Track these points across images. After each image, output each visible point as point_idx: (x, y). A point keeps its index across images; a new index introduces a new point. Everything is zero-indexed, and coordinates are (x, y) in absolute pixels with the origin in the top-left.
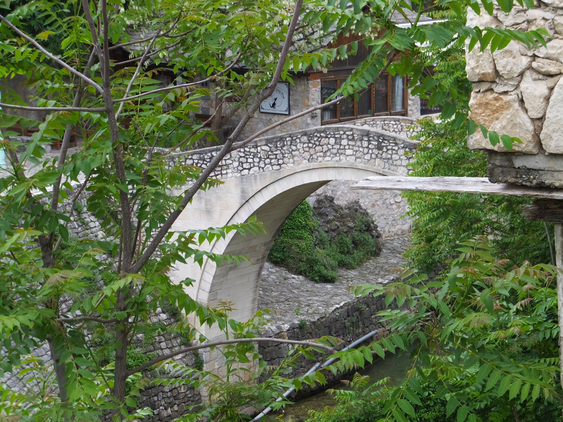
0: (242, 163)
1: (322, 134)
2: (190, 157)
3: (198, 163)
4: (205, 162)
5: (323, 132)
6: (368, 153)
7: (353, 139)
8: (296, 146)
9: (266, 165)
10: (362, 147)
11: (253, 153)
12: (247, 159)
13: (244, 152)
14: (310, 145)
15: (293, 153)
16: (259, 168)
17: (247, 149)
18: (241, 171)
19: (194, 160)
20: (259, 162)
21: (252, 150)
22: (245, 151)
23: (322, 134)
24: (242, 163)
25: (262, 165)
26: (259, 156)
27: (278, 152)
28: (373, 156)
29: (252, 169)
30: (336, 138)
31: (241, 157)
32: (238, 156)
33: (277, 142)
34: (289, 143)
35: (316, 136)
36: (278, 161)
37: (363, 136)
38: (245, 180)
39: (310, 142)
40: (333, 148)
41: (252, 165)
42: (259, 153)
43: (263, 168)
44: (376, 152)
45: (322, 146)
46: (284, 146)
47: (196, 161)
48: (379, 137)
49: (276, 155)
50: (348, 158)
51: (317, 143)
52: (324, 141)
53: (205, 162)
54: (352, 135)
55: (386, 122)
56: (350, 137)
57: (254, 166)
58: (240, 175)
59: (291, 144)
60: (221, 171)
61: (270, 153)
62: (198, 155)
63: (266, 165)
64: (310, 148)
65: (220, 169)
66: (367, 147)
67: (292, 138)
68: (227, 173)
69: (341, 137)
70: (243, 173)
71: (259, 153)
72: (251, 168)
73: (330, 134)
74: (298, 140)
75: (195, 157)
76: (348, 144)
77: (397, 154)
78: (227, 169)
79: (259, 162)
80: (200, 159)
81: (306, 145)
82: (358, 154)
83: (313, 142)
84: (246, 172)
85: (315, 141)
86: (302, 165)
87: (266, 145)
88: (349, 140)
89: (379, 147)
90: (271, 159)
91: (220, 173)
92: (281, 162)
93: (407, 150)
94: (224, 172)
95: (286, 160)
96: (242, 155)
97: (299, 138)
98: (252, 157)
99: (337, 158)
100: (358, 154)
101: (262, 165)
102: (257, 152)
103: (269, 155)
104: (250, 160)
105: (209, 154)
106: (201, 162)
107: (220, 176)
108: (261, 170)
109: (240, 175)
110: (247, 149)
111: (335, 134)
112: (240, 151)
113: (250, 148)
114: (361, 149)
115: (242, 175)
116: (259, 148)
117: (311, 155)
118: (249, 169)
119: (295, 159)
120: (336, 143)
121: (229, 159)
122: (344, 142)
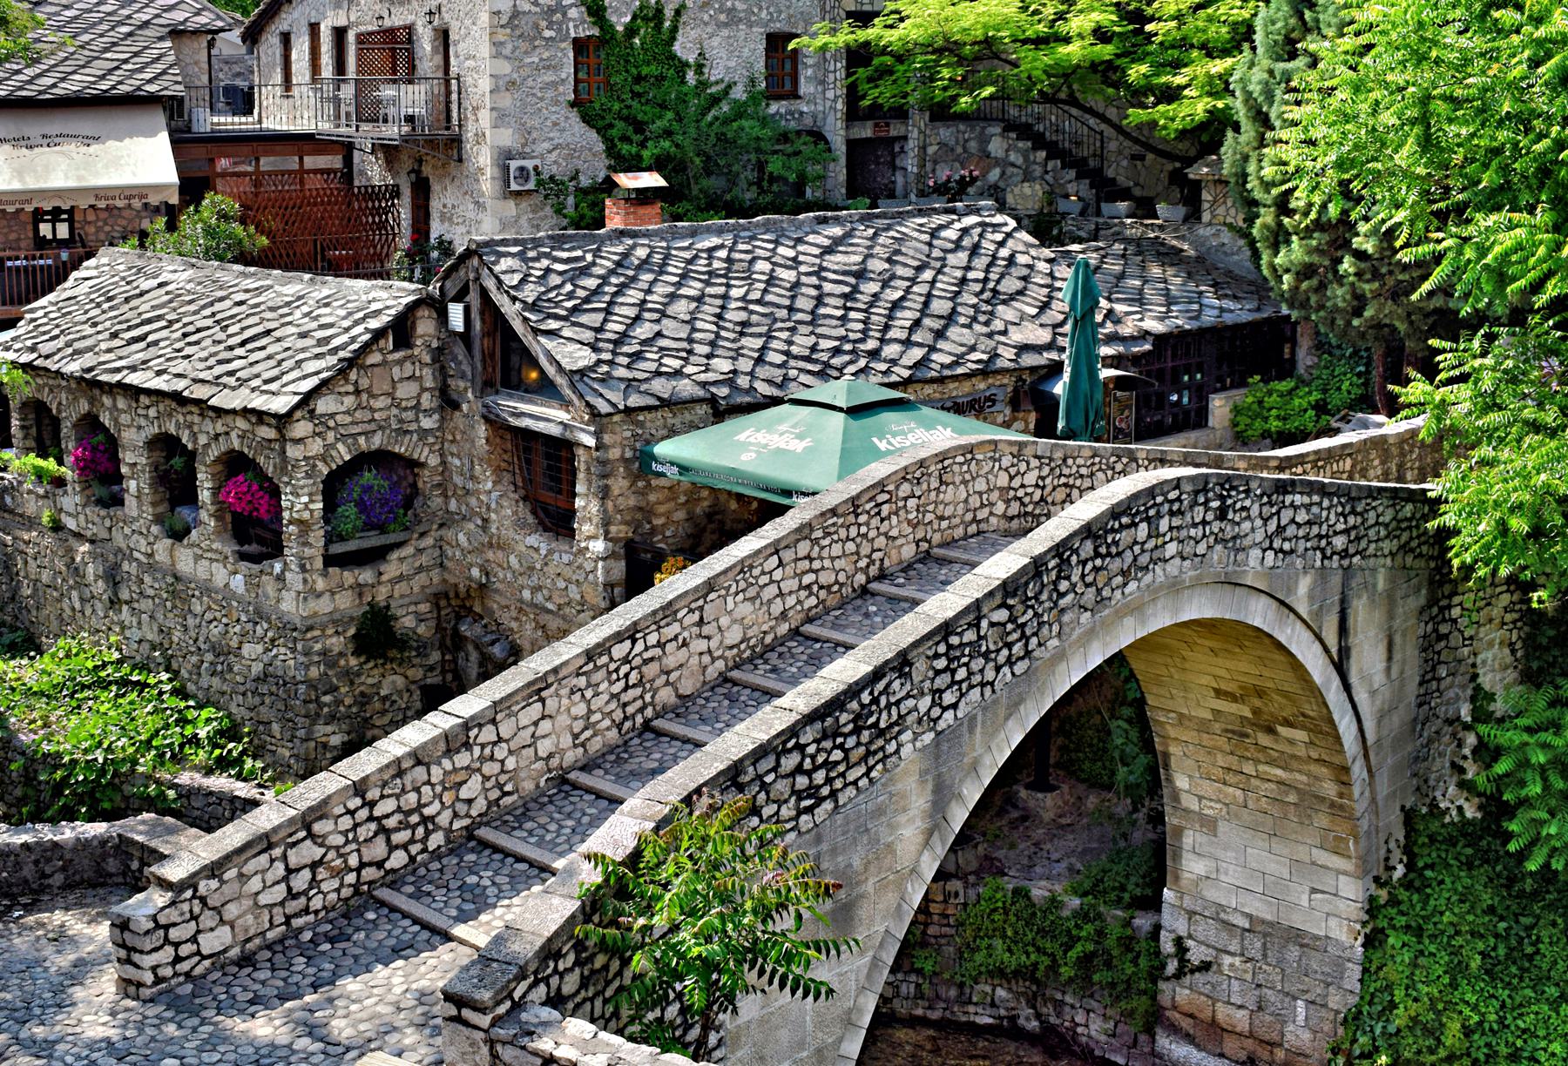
0: (941, 691)
1: (1125, 520)
2: (790, 745)
3: (818, 750)
4: (839, 740)
5: (1124, 513)
6: (1204, 536)
7: (1180, 512)
8: (1068, 578)
9: (998, 669)
10: (1195, 525)
11: (970, 644)
12: (953, 672)
13: (946, 654)
14: (1098, 562)
15: (1063, 602)
16: (983, 685)
17: (954, 640)
18: (936, 721)
19: (801, 748)
20: (982, 671)
21: (970, 636)
22: (950, 647)
23: (1125, 520)
24: (941, 691)
25: (990, 675)
26: (984, 648)
27: (1030, 612)
28: (1212, 539)
29: (962, 704)
30: (1148, 519)
31: (938, 672)
32: (931, 674)
33: (1027, 584)
34: (1053, 575)
35: (1113, 530)
36: (1026, 645)
37: (1196, 493)
38: (945, 747)
39: (1097, 555)
40: (1143, 551)
41: (964, 686)
42: (985, 637)
43: (992, 684)
44: (1216, 526)
45: (1119, 554)
46: (1043, 586)
47: (811, 749)
48: (1222, 486)
49: (1024, 625)
50: (1168, 567)
51: (1114, 550)
52: (1125, 537)
53: (839, 740)
54: (1179, 499)
55: (946, 463)
56: (1176, 507)
57: (971, 687)
58: (932, 735)
59: (1059, 577)
60: (882, 748)
61: (1010, 627)
62: (818, 725)
63: (998, 669)
64: (1096, 569)
65: (880, 742)
66: (1204, 523)
67: (1059, 555)
68: (900, 746)
69: (1158, 512)
70: (942, 725)
71: (985, 637)
72: (962, 695)
73: (1138, 512)
74: (1074, 558)
75: (808, 736)
76: (1171, 528)
77: (1248, 517)
78: (899, 733)
79: (982, 671)
80: (825, 737)
81: (1089, 566)
82: (1188, 549)
83: (1103, 550)
84: (949, 715)
85: (1108, 546)
86: (1078, 632)
87: (1003, 605)
88: (1172, 513)
89: (1222, 514)
90: (1009, 646)
91: (880, 755)
92: (1034, 641)
93: (1265, 499)
94: (891, 748)
95: (1045, 630)
96: (941, 663)
97: (1076, 551)
98: (965, 660)
99: (1148, 578)
100: (1188, 549)
101: (990, 675)
102: (980, 638)
103: (1009, 634)
104: (962, 673)
105: (854, 705)
106: (827, 744)
107: (879, 767)
108: (988, 690)
109: (932, 735)
110: (954, 640)
111: (1147, 510)
112: (937, 656)
113: (960, 634)
114: (1193, 532)
115: (938, 734)
116: (984, 624)
117: (1099, 591)
118: (955, 706)
119: (1066, 618)
120: (1149, 536)
121: (908, 696)
122: (1164, 525)
